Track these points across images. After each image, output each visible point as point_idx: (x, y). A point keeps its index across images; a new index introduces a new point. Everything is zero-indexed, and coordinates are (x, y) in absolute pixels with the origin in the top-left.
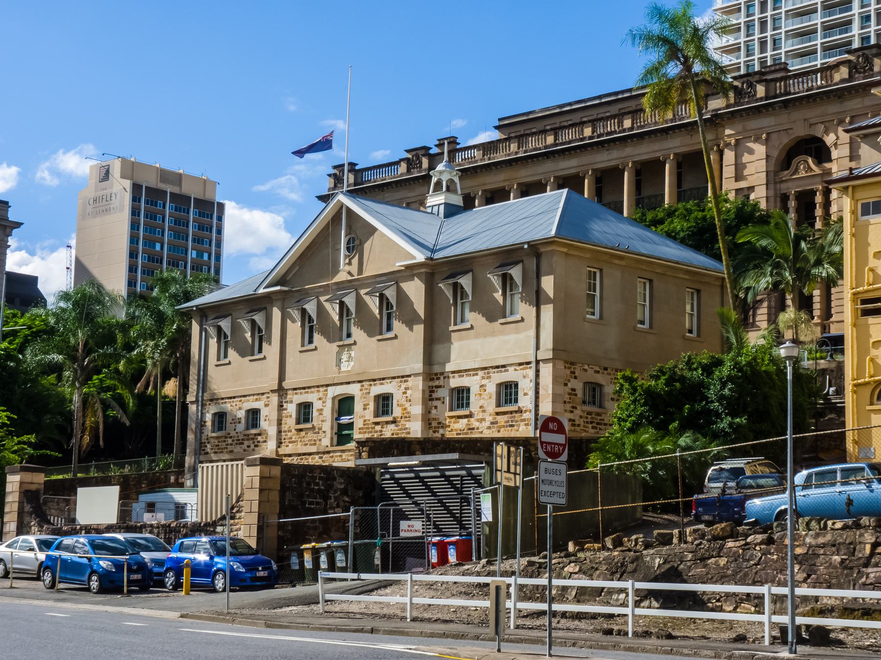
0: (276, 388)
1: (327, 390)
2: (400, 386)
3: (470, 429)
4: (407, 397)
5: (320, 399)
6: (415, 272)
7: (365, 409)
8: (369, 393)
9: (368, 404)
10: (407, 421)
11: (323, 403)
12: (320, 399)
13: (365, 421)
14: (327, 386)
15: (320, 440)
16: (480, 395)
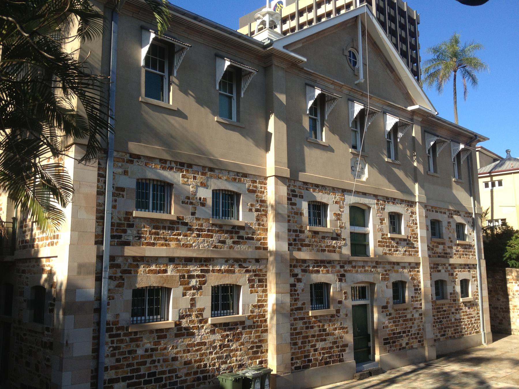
0: (288, 176)
1: (344, 196)
2: (407, 210)
3: (445, 253)
4: (413, 220)
5: (336, 202)
6: (415, 117)
7: (381, 223)
8: (384, 209)
9: (384, 220)
10: (415, 241)
11: (340, 207)
12: (336, 202)
13: (383, 235)
14: (344, 191)
15: (340, 248)
16: (449, 229)
